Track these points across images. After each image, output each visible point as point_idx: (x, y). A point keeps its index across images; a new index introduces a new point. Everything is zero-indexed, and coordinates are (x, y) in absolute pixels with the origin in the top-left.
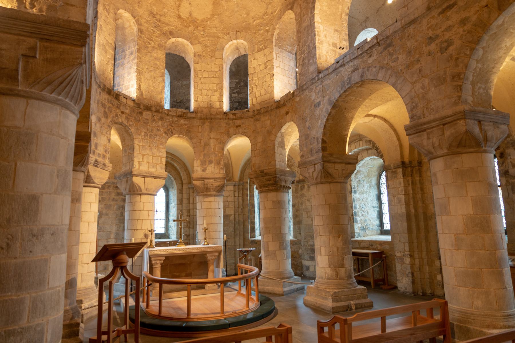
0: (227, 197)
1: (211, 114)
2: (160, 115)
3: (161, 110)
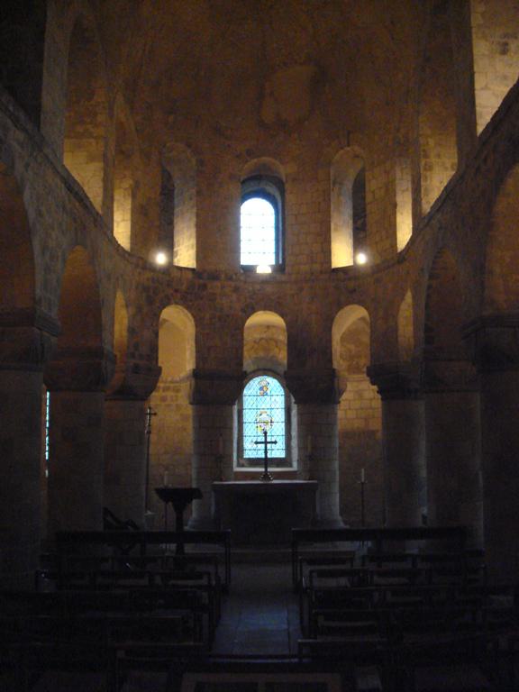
0: (371, 400)
1: (312, 274)
2: (233, 284)
3: (234, 277)
